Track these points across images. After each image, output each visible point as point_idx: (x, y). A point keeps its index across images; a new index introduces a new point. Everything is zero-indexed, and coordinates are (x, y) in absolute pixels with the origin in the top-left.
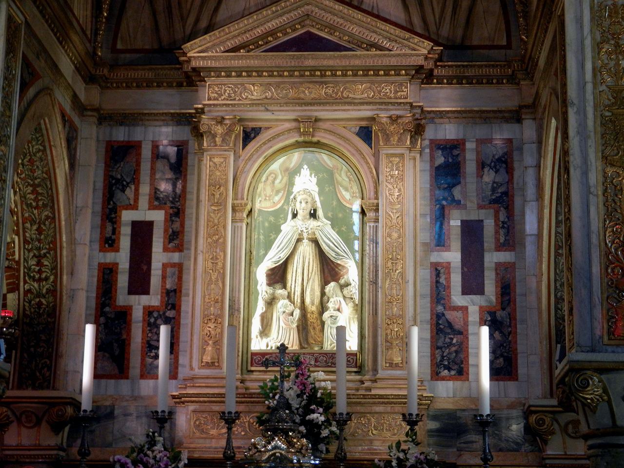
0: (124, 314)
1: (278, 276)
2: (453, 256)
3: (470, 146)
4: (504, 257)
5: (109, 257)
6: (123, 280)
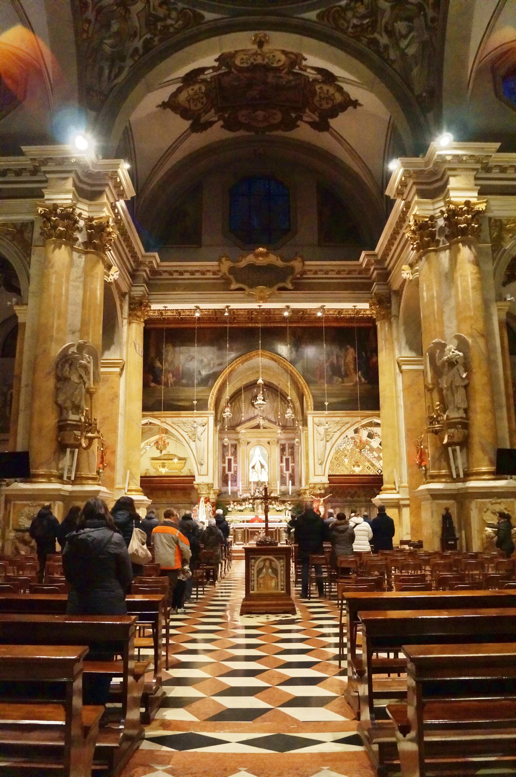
0: (227, 475)
1: (253, 467)
2: (284, 464)
3: (287, 445)
4: (293, 464)
5: (224, 465)
6: (227, 469)
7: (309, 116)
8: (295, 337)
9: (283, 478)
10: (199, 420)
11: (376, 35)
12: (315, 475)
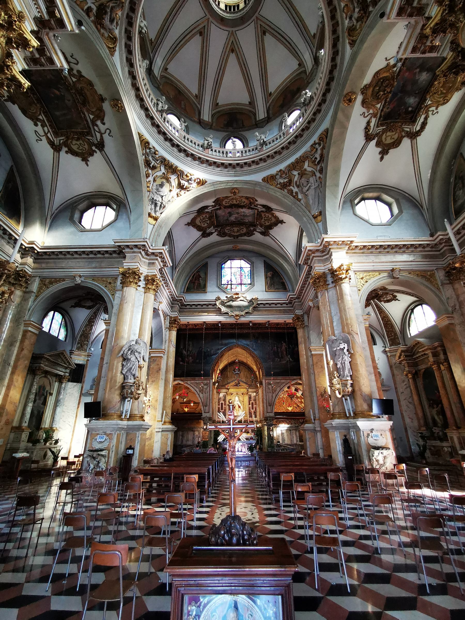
2: (251, 406)
7: (259, 229)
8: (255, 337)
9: (250, 413)
10: (205, 382)
11: (291, 187)
12: (267, 412)
